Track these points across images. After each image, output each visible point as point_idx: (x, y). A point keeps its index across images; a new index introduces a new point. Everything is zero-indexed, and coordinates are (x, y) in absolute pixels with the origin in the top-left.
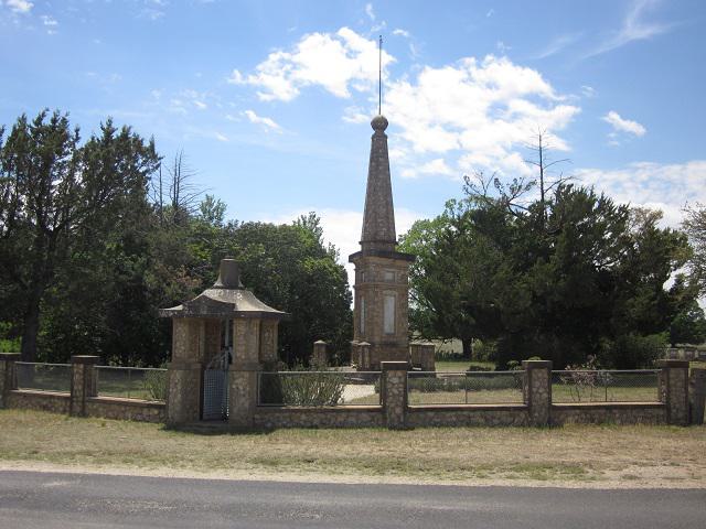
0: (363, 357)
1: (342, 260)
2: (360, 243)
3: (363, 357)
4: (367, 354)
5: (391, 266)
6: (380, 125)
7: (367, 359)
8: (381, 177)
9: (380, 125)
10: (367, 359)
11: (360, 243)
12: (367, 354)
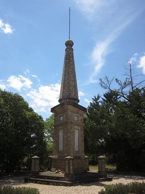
0: (69, 168)
1: (144, 53)
2: (53, 110)
3: (69, 168)
4: (71, 164)
5: (77, 113)
6: (69, 44)
7: (71, 167)
8: (71, 67)
9: (69, 44)
10: (71, 167)
11: (53, 110)
12: (71, 164)
